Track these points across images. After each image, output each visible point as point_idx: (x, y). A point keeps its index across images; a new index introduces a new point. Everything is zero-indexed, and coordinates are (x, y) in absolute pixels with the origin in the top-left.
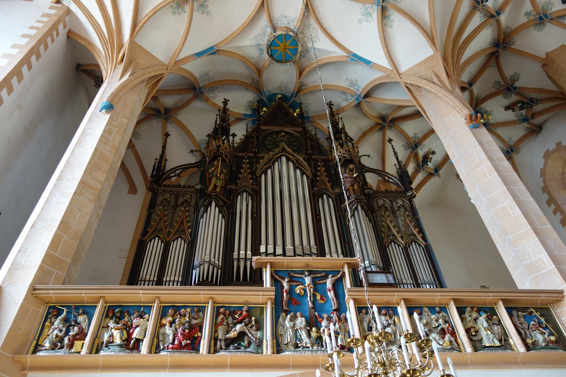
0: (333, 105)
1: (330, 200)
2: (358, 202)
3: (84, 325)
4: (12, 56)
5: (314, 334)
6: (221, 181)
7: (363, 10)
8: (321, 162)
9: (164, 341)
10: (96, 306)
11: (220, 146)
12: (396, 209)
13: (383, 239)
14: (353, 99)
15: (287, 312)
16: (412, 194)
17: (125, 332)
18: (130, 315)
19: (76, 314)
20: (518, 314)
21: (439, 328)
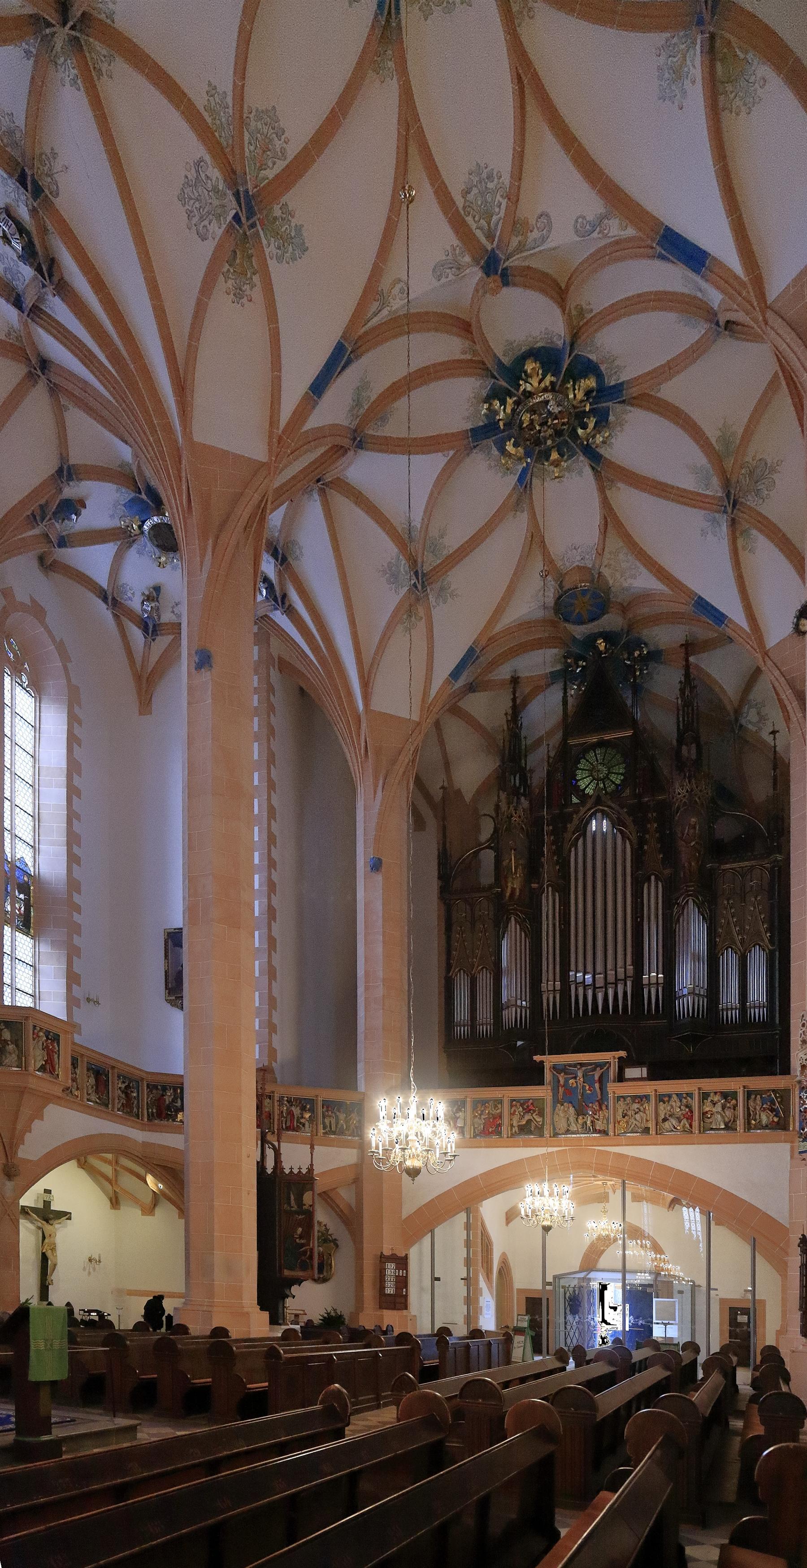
5: (580, 1121)
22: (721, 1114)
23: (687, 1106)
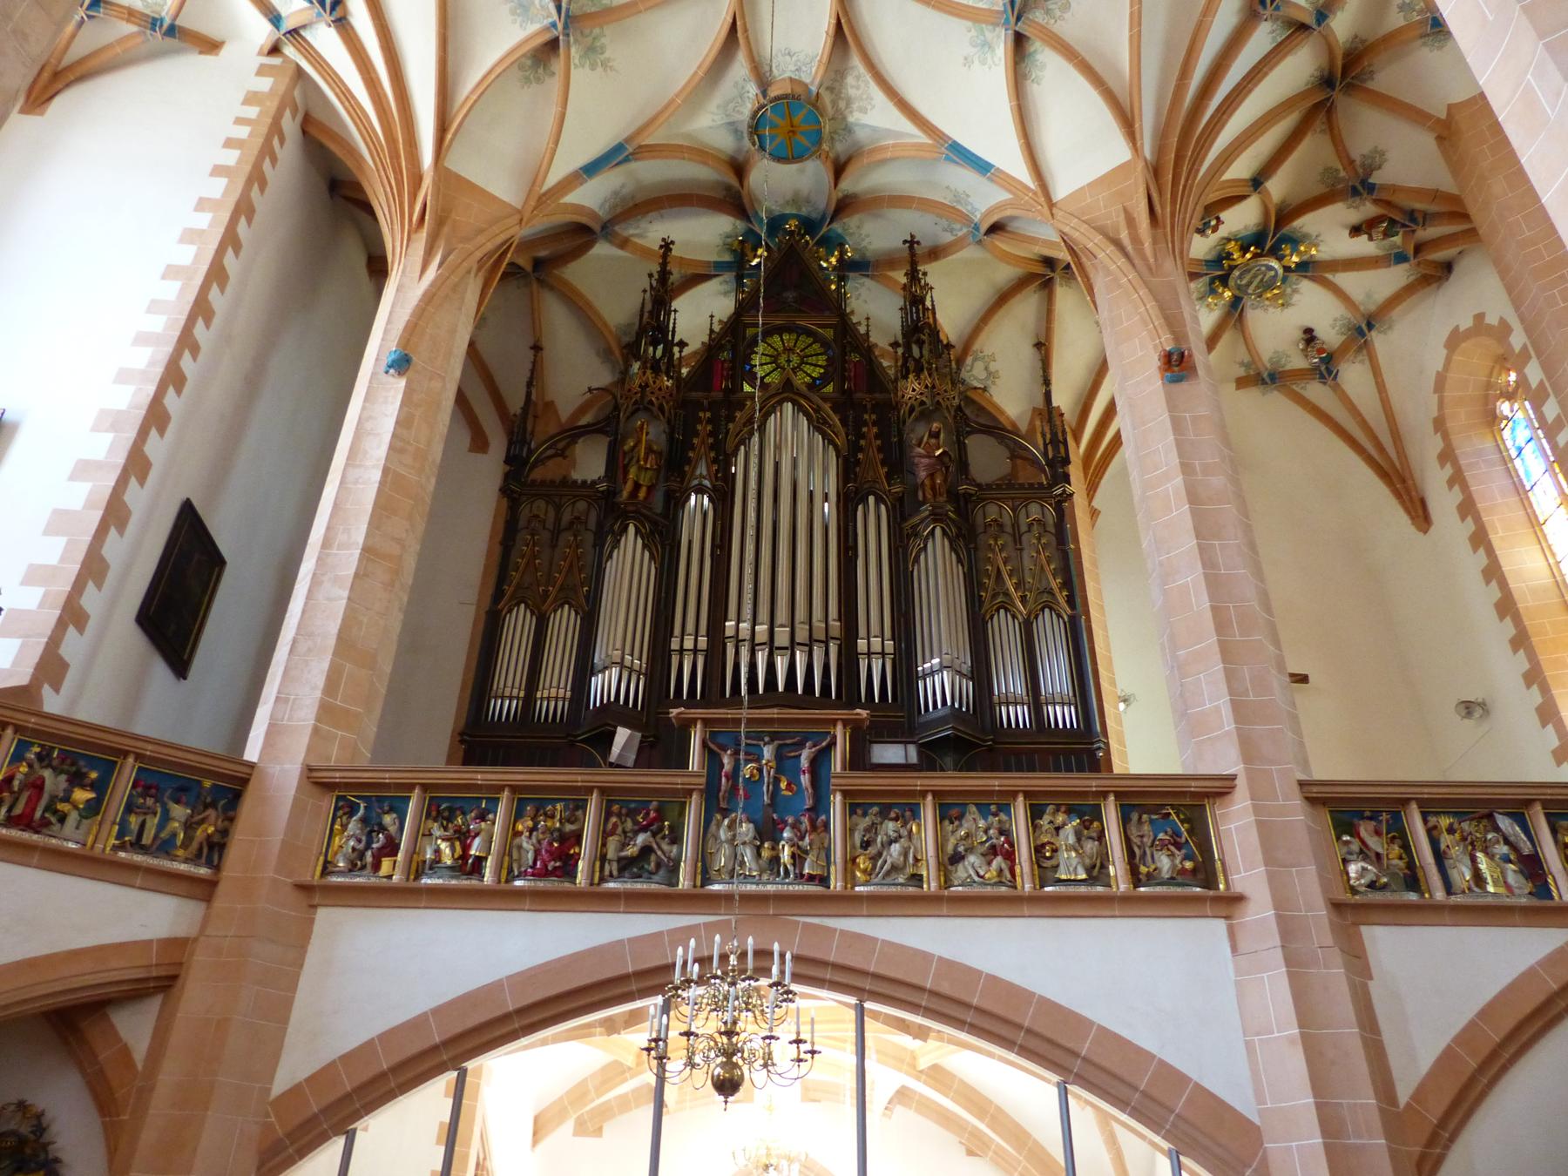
0: (918, 243)
1: (883, 507)
2: (935, 521)
3: (393, 829)
4: (201, 233)
5: (766, 854)
6: (650, 473)
7: (973, 33)
8: (874, 413)
9: (519, 860)
10: (409, 798)
11: (647, 385)
12: (1024, 528)
13: (981, 603)
14: (965, 230)
15: (725, 813)
16: (1064, 491)
17: (457, 844)
18: (464, 814)
19: (380, 811)
20: (1140, 818)
21: (987, 845)
22: (1076, 851)
23: (1002, 832)
